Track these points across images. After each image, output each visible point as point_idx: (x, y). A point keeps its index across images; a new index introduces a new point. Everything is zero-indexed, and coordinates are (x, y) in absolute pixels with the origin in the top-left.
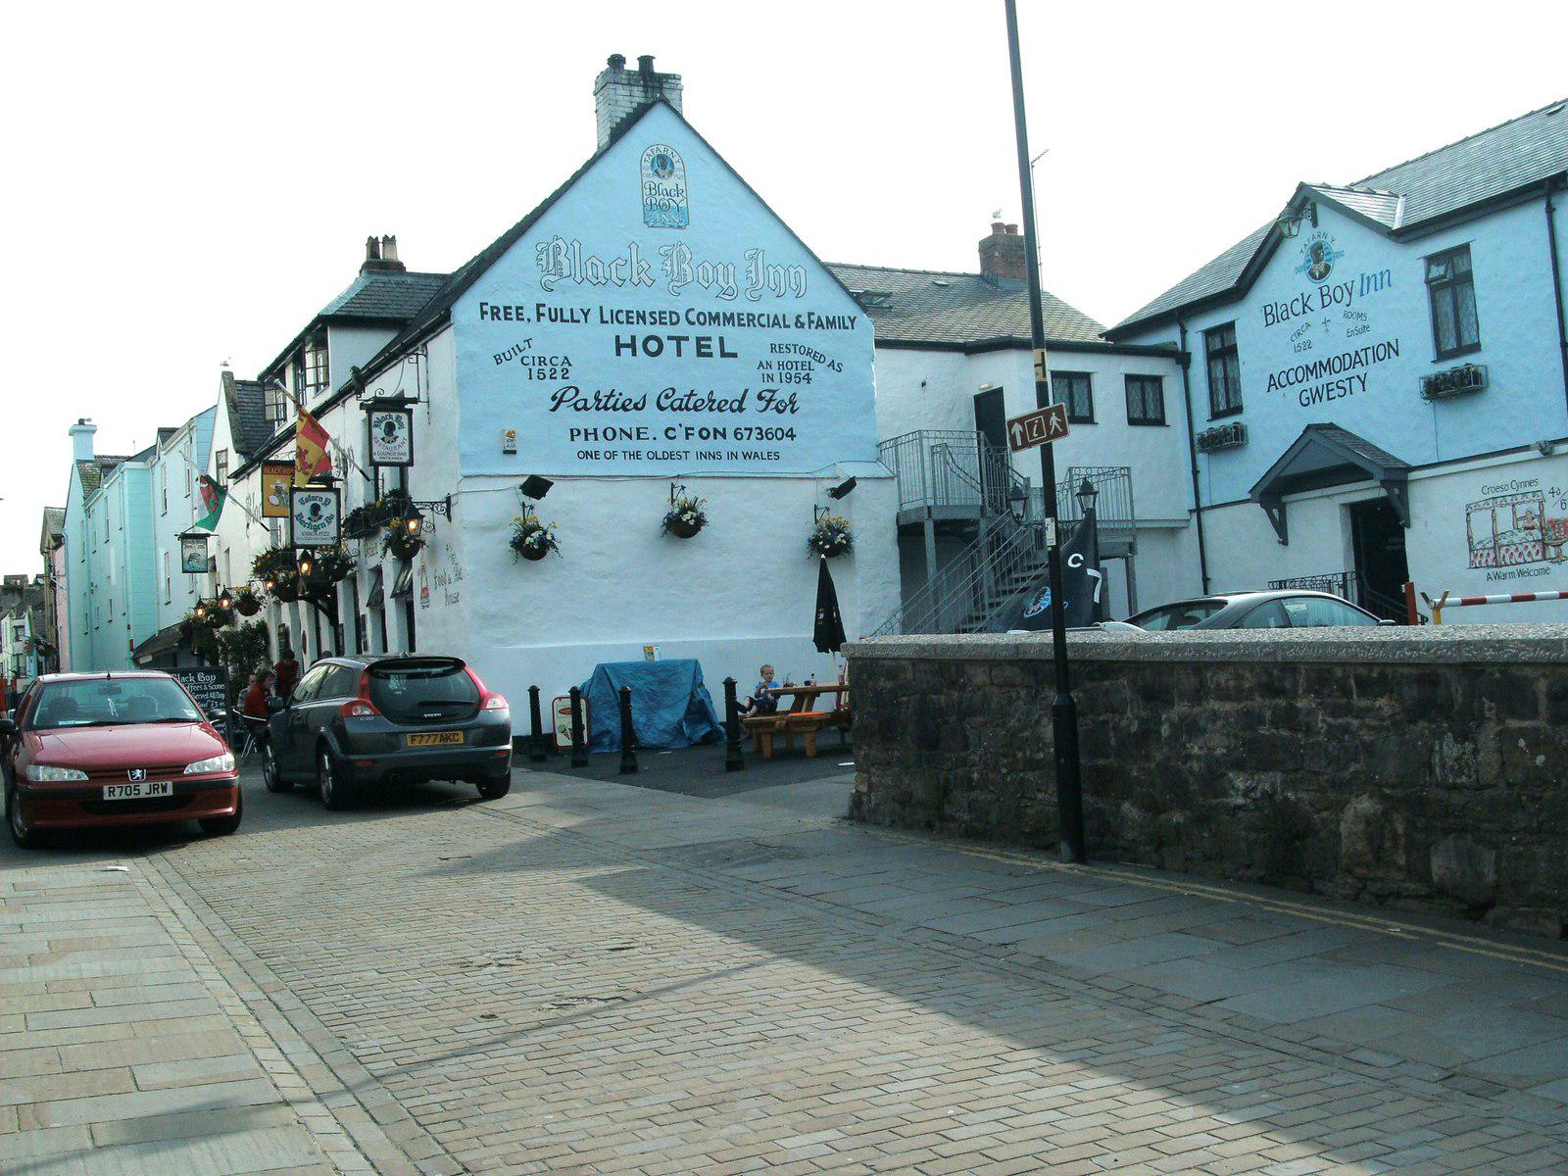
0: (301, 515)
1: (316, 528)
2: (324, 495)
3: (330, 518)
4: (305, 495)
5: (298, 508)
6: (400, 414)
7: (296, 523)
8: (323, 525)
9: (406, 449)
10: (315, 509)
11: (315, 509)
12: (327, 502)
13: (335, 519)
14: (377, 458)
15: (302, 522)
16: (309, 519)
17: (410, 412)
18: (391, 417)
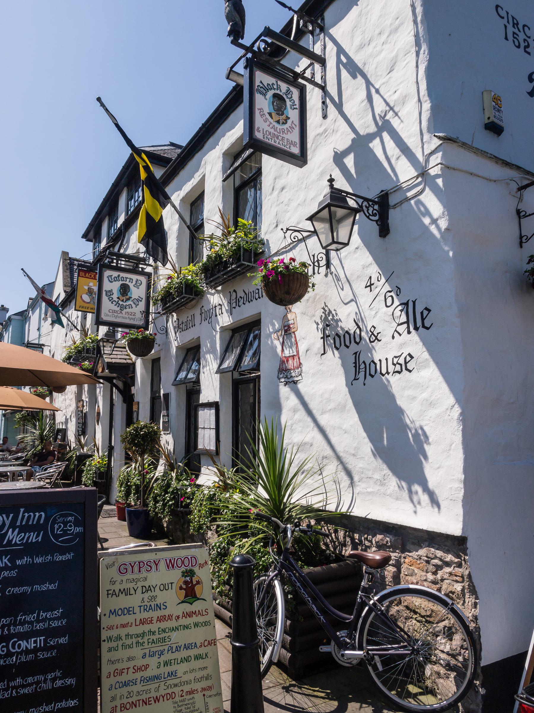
0: (111, 291)
1: (122, 308)
2: (134, 277)
3: (139, 300)
4: (115, 274)
5: (107, 286)
6: (292, 89)
7: (105, 298)
8: (130, 306)
9: (295, 136)
10: (125, 290)
11: (125, 290)
12: (138, 284)
13: (144, 300)
14: (259, 135)
15: (111, 300)
16: (118, 298)
17: (302, 91)
18: (279, 88)
